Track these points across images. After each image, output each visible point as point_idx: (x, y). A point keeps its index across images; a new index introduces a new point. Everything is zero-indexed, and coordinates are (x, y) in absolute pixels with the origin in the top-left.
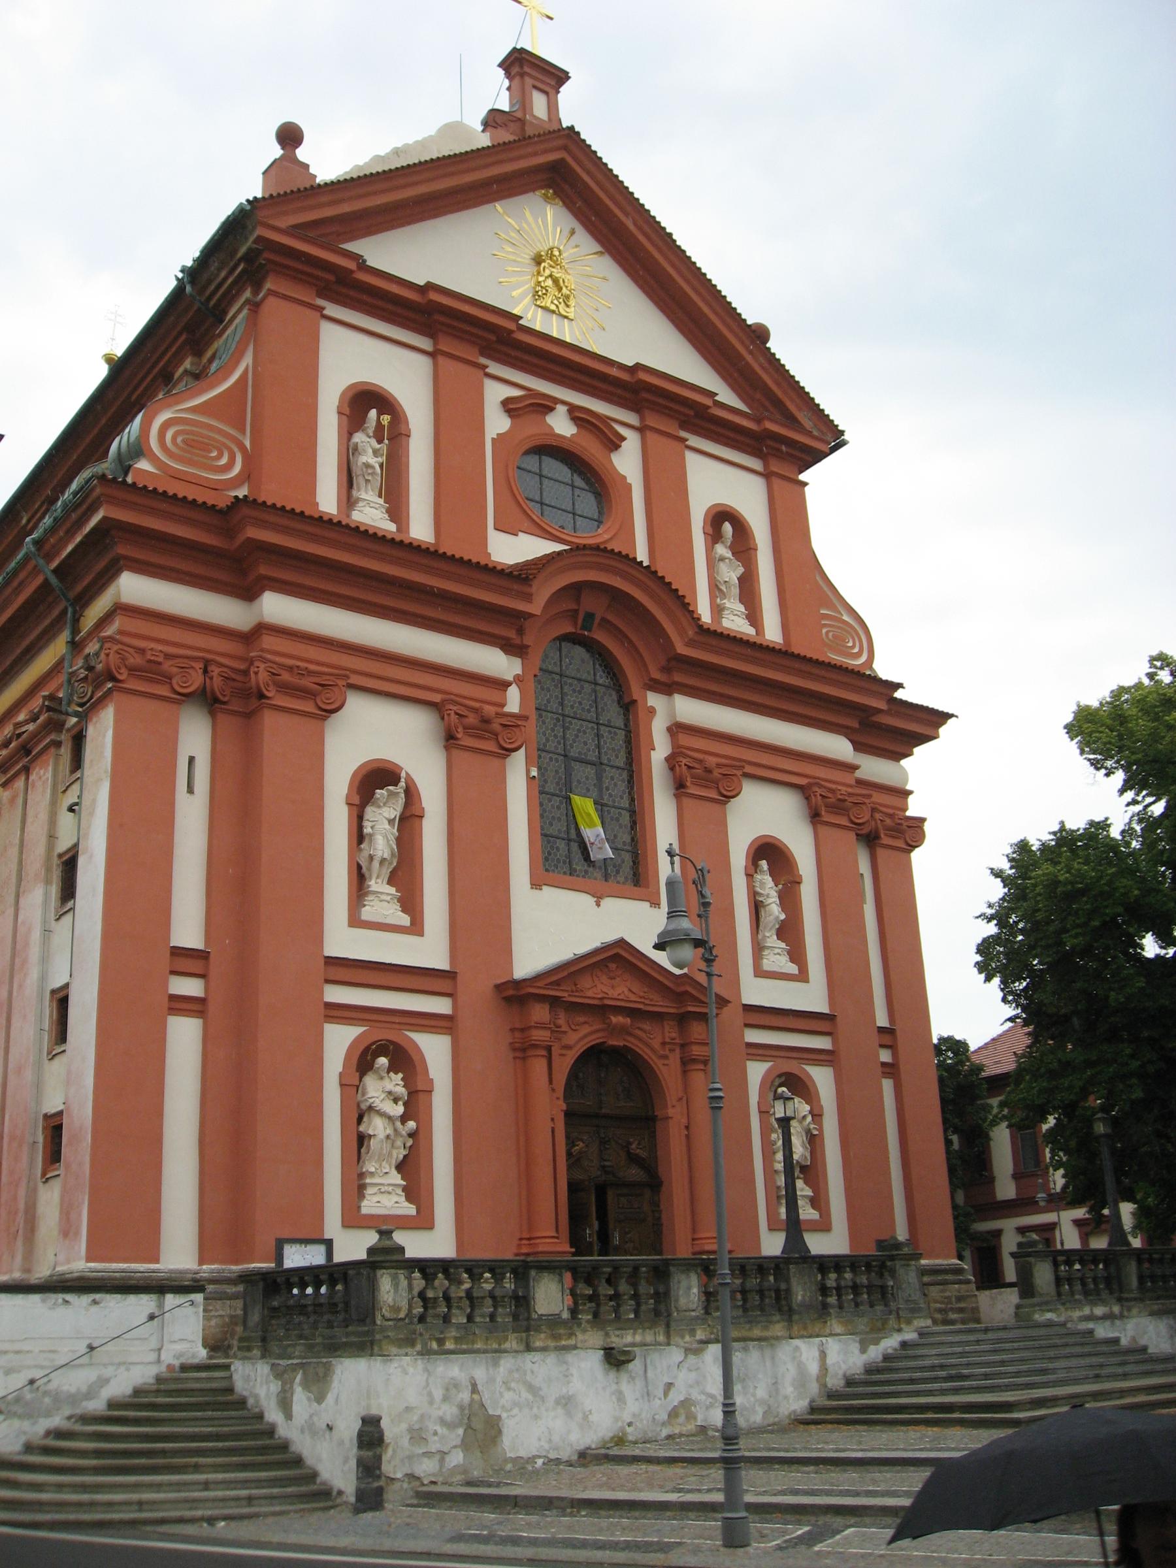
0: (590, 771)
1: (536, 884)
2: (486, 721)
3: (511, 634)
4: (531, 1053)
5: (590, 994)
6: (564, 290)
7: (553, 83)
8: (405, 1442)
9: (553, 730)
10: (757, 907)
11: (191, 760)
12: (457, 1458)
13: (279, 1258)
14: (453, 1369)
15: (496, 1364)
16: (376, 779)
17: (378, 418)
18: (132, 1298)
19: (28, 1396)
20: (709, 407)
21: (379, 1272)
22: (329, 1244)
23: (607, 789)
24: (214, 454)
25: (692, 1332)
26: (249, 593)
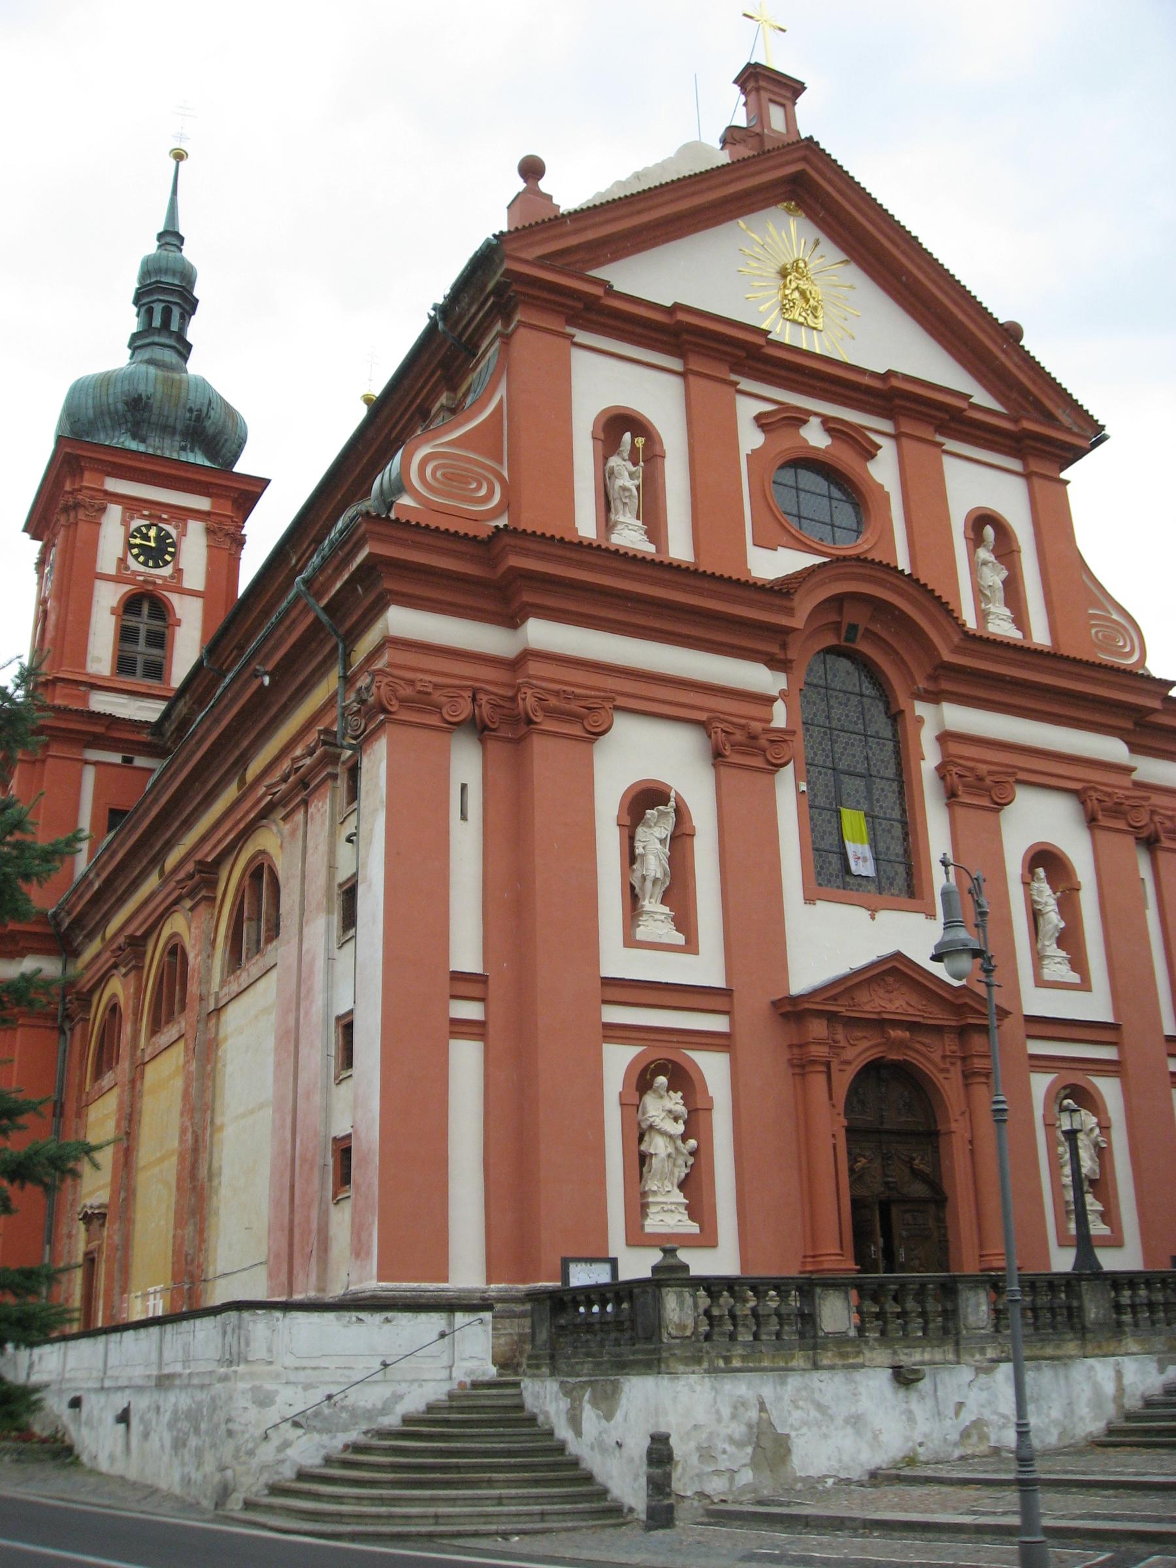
0: (860, 783)
1: (809, 899)
2: (753, 737)
3: (774, 649)
4: (808, 1069)
5: (867, 1008)
6: (812, 302)
7: (789, 95)
8: (694, 1459)
9: (820, 743)
10: (1035, 916)
11: (464, 787)
12: (746, 1477)
13: (565, 1277)
14: (741, 1388)
15: (783, 1383)
16: (645, 799)
17: (633, 441)
18: (423, 1317)
19: (327, 1411)
20: (965, 410)
21: (665, 1290)
22: (613, 1262)
23: (878, 800)
24: (474, 486)
25: (982, 1351)
26: (512, 621)
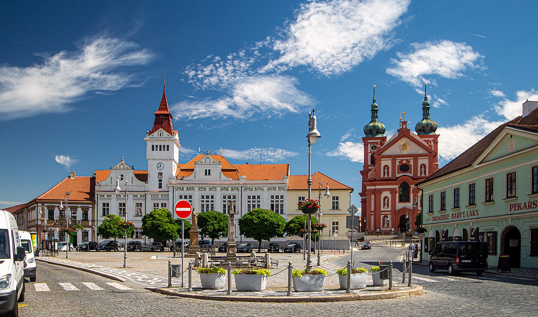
16: (385, 197)
